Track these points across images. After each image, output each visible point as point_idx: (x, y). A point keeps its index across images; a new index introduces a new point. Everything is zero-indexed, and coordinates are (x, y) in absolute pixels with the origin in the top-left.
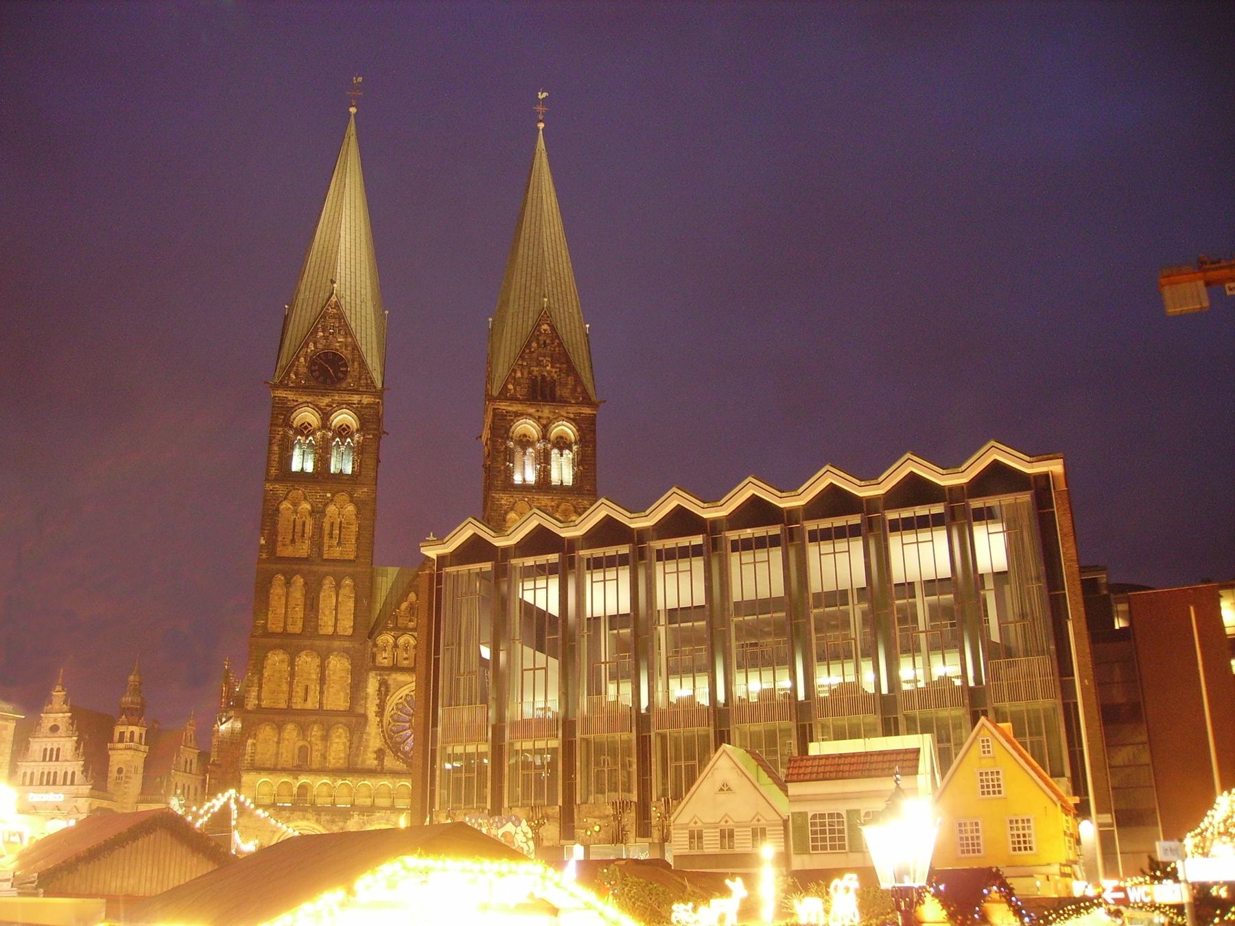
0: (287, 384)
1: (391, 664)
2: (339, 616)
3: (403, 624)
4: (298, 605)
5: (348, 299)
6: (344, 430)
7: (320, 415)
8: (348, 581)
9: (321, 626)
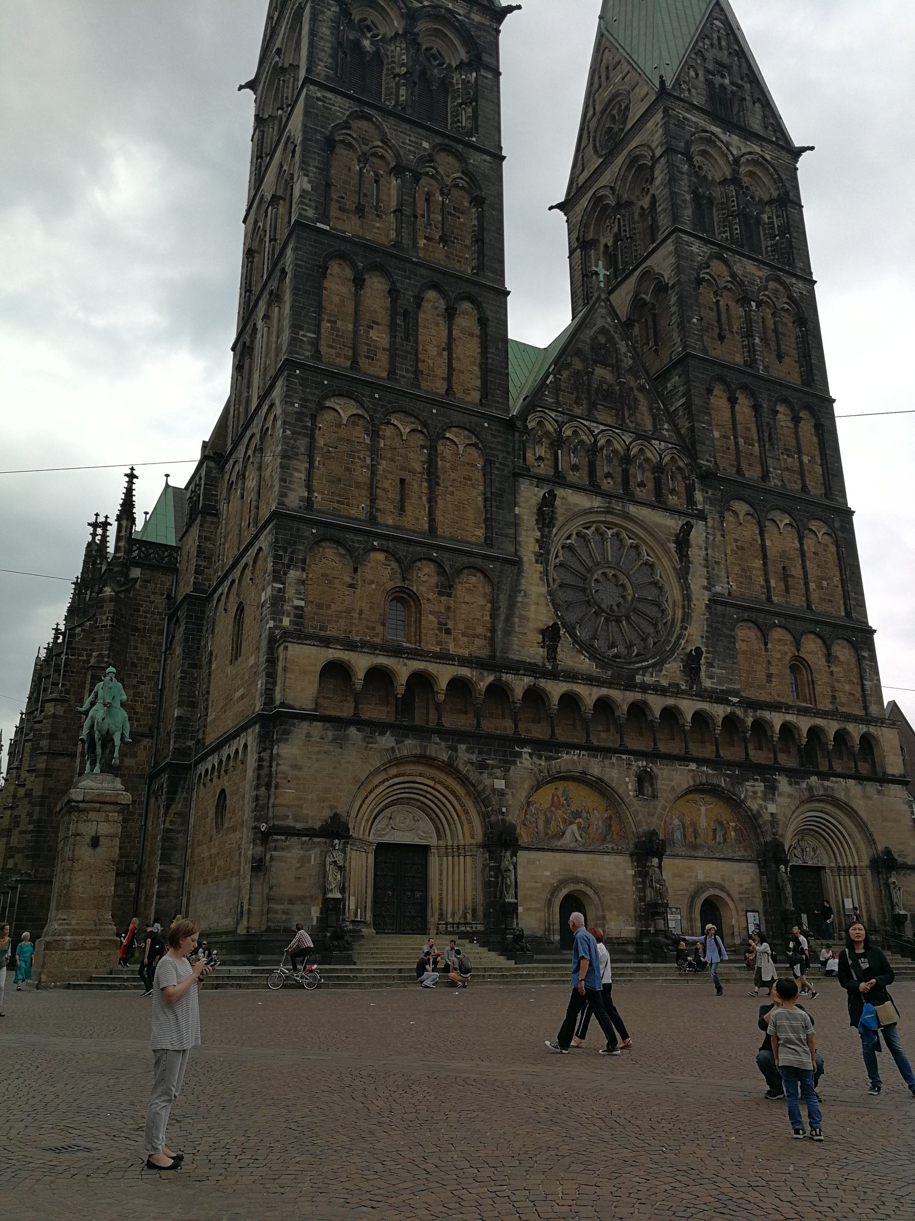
1: (551, 472)
2: (455, 364)
3: (565, 404)
4: (378, 324)
6: (434, 56)
7: (400, 9)
8: (466, 306)
9: (422, 372)
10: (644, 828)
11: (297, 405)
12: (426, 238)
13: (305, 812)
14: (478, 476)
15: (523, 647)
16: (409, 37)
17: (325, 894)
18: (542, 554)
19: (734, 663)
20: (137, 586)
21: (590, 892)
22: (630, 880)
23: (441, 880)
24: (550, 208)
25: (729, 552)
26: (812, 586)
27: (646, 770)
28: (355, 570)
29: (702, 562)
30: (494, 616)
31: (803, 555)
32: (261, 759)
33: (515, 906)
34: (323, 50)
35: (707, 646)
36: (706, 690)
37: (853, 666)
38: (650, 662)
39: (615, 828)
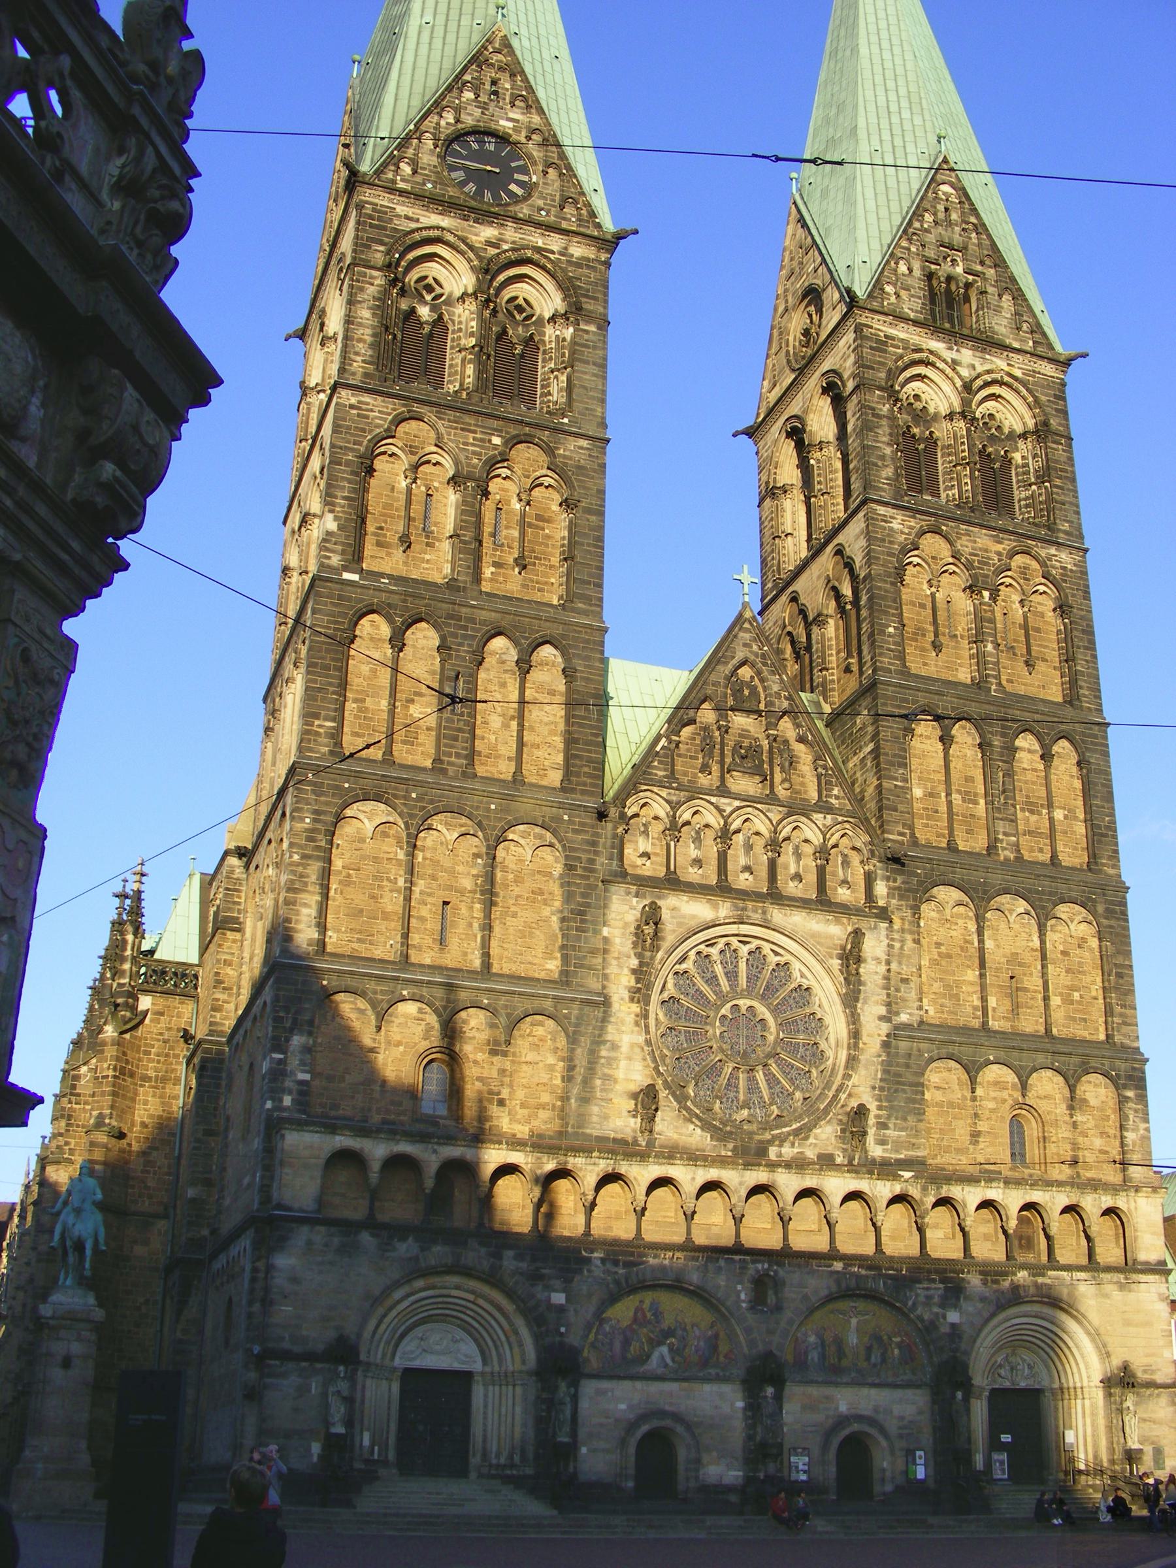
0: (394, 182)
1: (661, 872)
2: (527, 737)
3: (685, 774)
5: (526, 43)
6: (520, 309)
7: (469, 260)
10: (761, 1347)
11: (308, 820)
12: (496, 565)
13: (304, 1333)
14: (556, 889)
15: (606, 1117)
17: (328, 1428)
18: (639, 990)
19: (921, 1121)
20: (147, 1021)
21: (680, 1429)
22: (740, 1415)
23: (485, 1413)
24: (734, 435)
25: (925, 962)
26: (1055, 1001)
27: (768, 1275)
28: (379, 1028)
29: (881, 982)
30: (568, 1079)
31: (1044, 957)
32: (255, 1270)
33: (574, 1446)
34: (364, 341)
35: (880, 1100)
36: (873, 1161)
37: (1109, 1112)
38: (794, 1127)
39: (723, 1348)
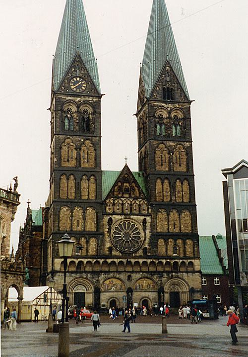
6: (86, 112)
10: (128, 287)
16: (78, 112)
39: (123, 287)
